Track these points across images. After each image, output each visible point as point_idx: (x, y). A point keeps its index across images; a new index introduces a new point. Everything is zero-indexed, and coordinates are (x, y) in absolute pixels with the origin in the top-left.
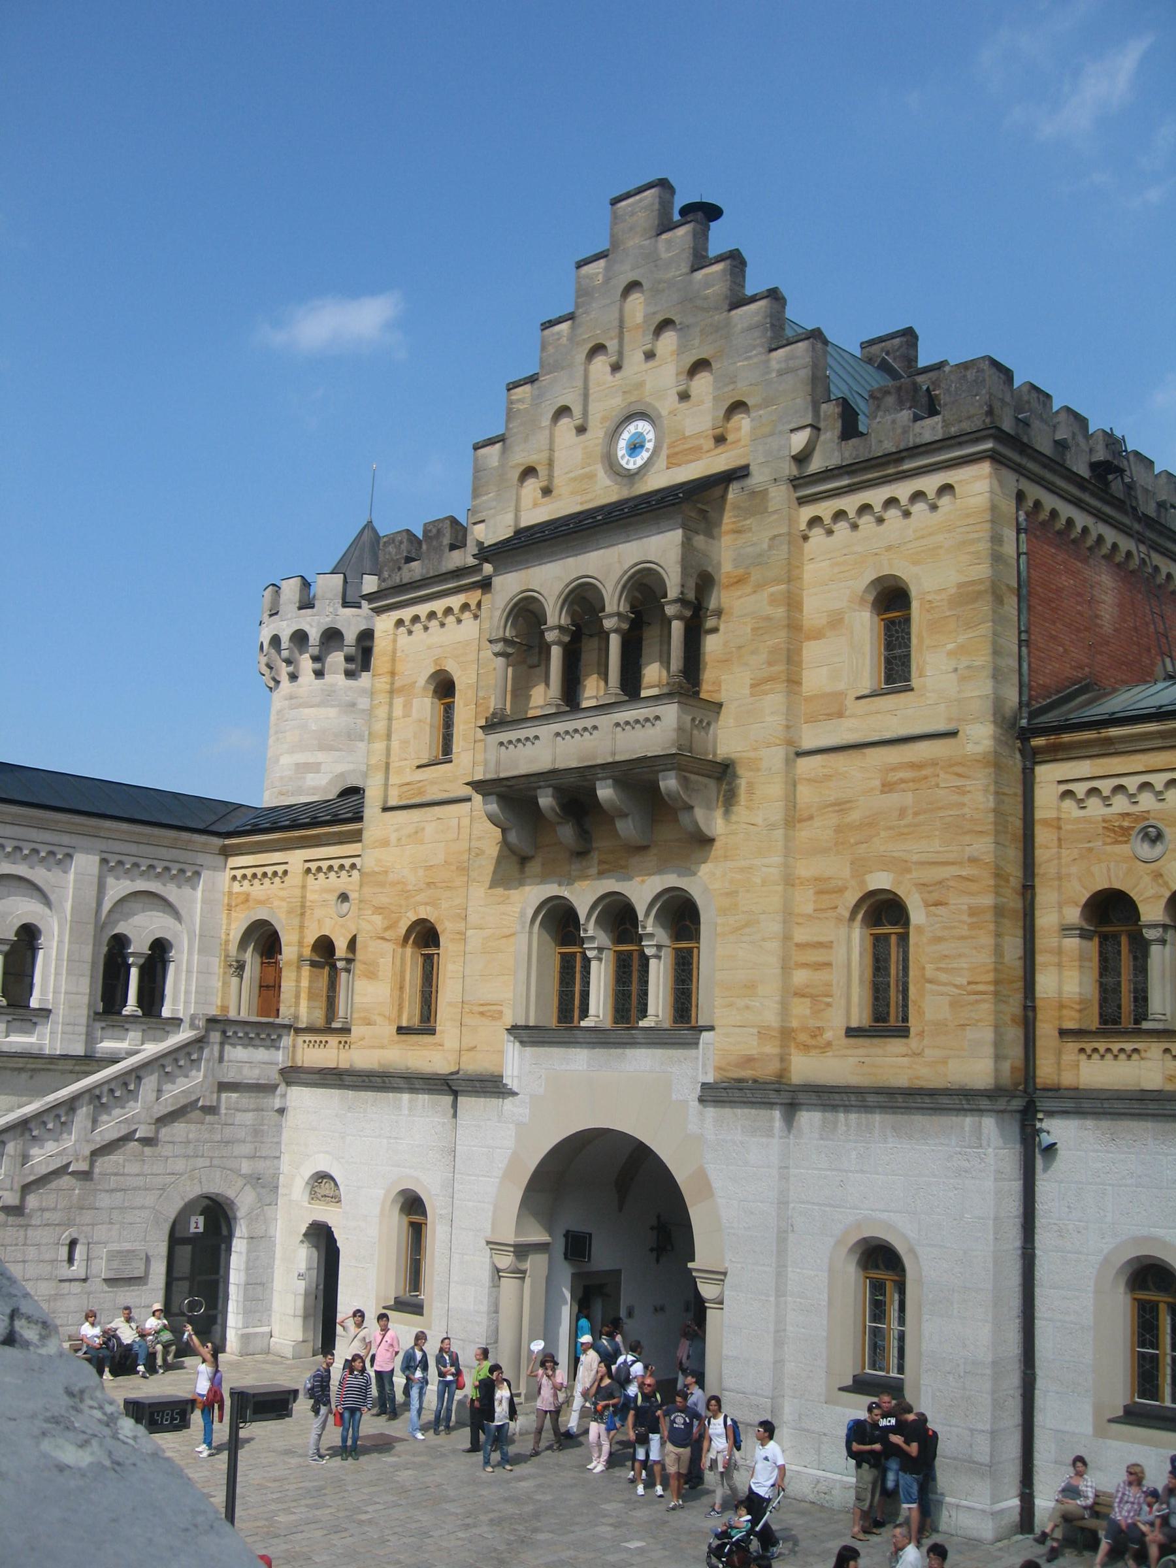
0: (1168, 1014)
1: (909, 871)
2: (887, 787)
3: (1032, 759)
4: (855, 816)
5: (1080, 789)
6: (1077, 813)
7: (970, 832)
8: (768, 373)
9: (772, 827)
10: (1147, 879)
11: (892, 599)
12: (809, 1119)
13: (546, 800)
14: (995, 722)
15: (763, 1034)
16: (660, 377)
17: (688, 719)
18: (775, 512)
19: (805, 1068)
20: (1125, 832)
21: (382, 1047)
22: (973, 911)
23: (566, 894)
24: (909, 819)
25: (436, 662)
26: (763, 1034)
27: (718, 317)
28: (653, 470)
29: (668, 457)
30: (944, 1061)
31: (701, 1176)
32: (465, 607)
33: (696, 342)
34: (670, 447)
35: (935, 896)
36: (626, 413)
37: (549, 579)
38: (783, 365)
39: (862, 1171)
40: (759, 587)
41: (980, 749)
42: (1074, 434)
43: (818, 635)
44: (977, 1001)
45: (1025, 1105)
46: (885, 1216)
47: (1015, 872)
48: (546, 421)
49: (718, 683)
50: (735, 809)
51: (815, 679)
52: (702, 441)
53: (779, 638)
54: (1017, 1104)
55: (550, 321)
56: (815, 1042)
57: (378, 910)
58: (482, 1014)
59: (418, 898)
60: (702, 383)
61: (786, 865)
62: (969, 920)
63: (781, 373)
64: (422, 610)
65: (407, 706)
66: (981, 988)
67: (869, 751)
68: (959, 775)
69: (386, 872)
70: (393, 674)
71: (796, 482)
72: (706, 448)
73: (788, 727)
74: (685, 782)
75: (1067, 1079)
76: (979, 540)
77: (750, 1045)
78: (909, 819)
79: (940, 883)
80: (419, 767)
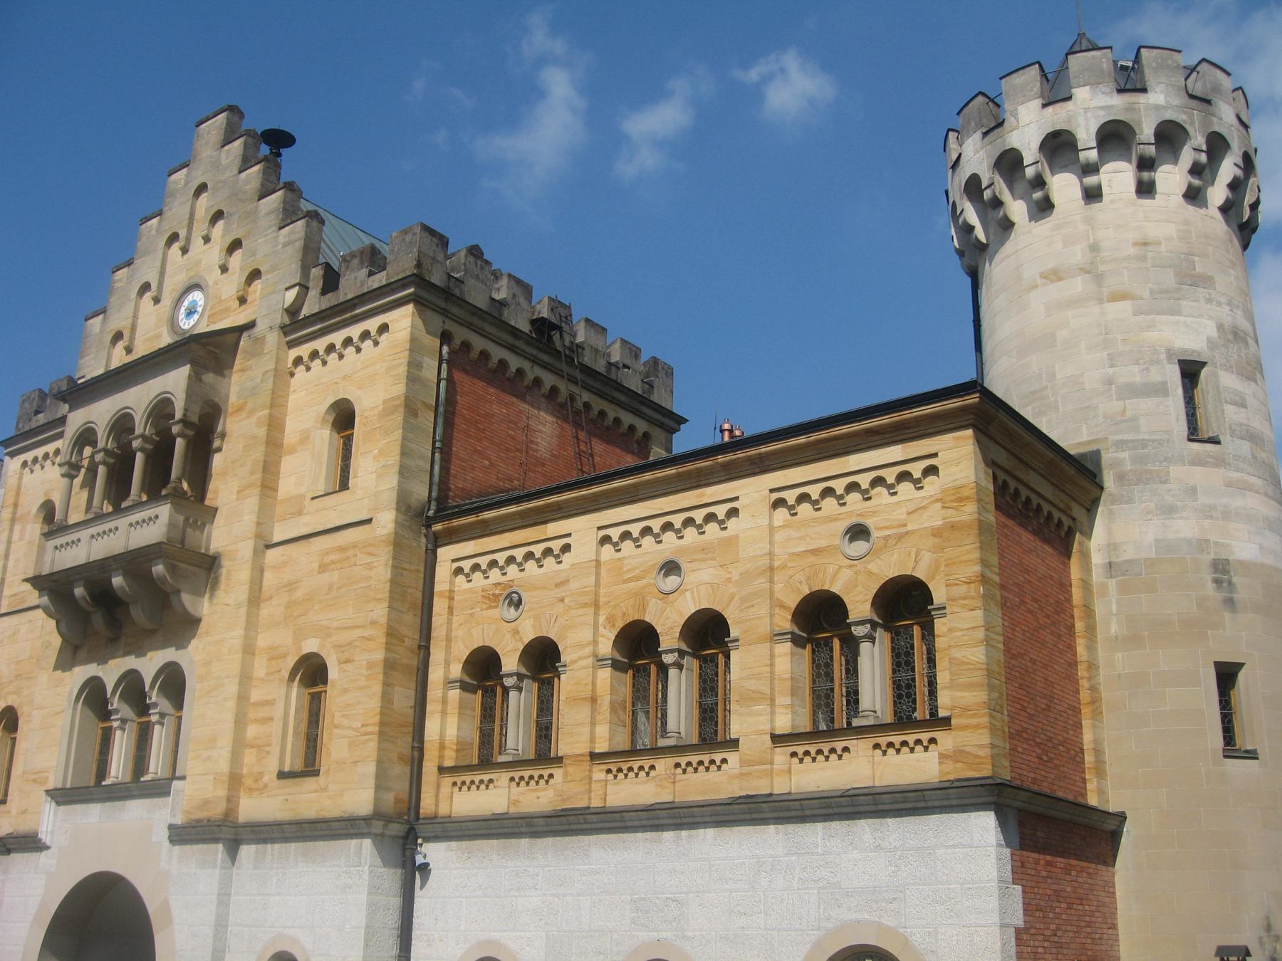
0: (520, 748)
1: (329, 636)
2: (323, 568)
3: (437, 541)
4: (299, 594)
6: (467, 586)
10: (508, 636)
12: (247, 852)
13: (79, 591)
14: (398, 510)
16: (207, 256)
17: (181, 518)
19: (251, 808)
22: (370, 666)
23: (100, 674)
25: (46, 494)
27: (250, 206)
31: (166, 905)
34: (212, 308)
36: (186, 285)
37: (100, 413)
39: (279, 894)
40: (251, 413)
41: (385, 532)
42: (514, 296)
44: (367, 741)
45: (403, 834)
47: (412, 636)
48: (134, 295)
49: (216, 492)
50: (217, 593)
51: (287, 485)
53: (259, 453)
54: (396, 829)
58: (34, 781)
60: (237, 259)
61: (246, 637)
62: (366, 673)
63: (285, 245)
65: (23, 531)
66: (370, 729)
67: (313, 540)
68: (370, 554)
70: (16, 505)
71: (285, 330)
73: (258, 524)
74: (172, 569)
75: (443, 810)
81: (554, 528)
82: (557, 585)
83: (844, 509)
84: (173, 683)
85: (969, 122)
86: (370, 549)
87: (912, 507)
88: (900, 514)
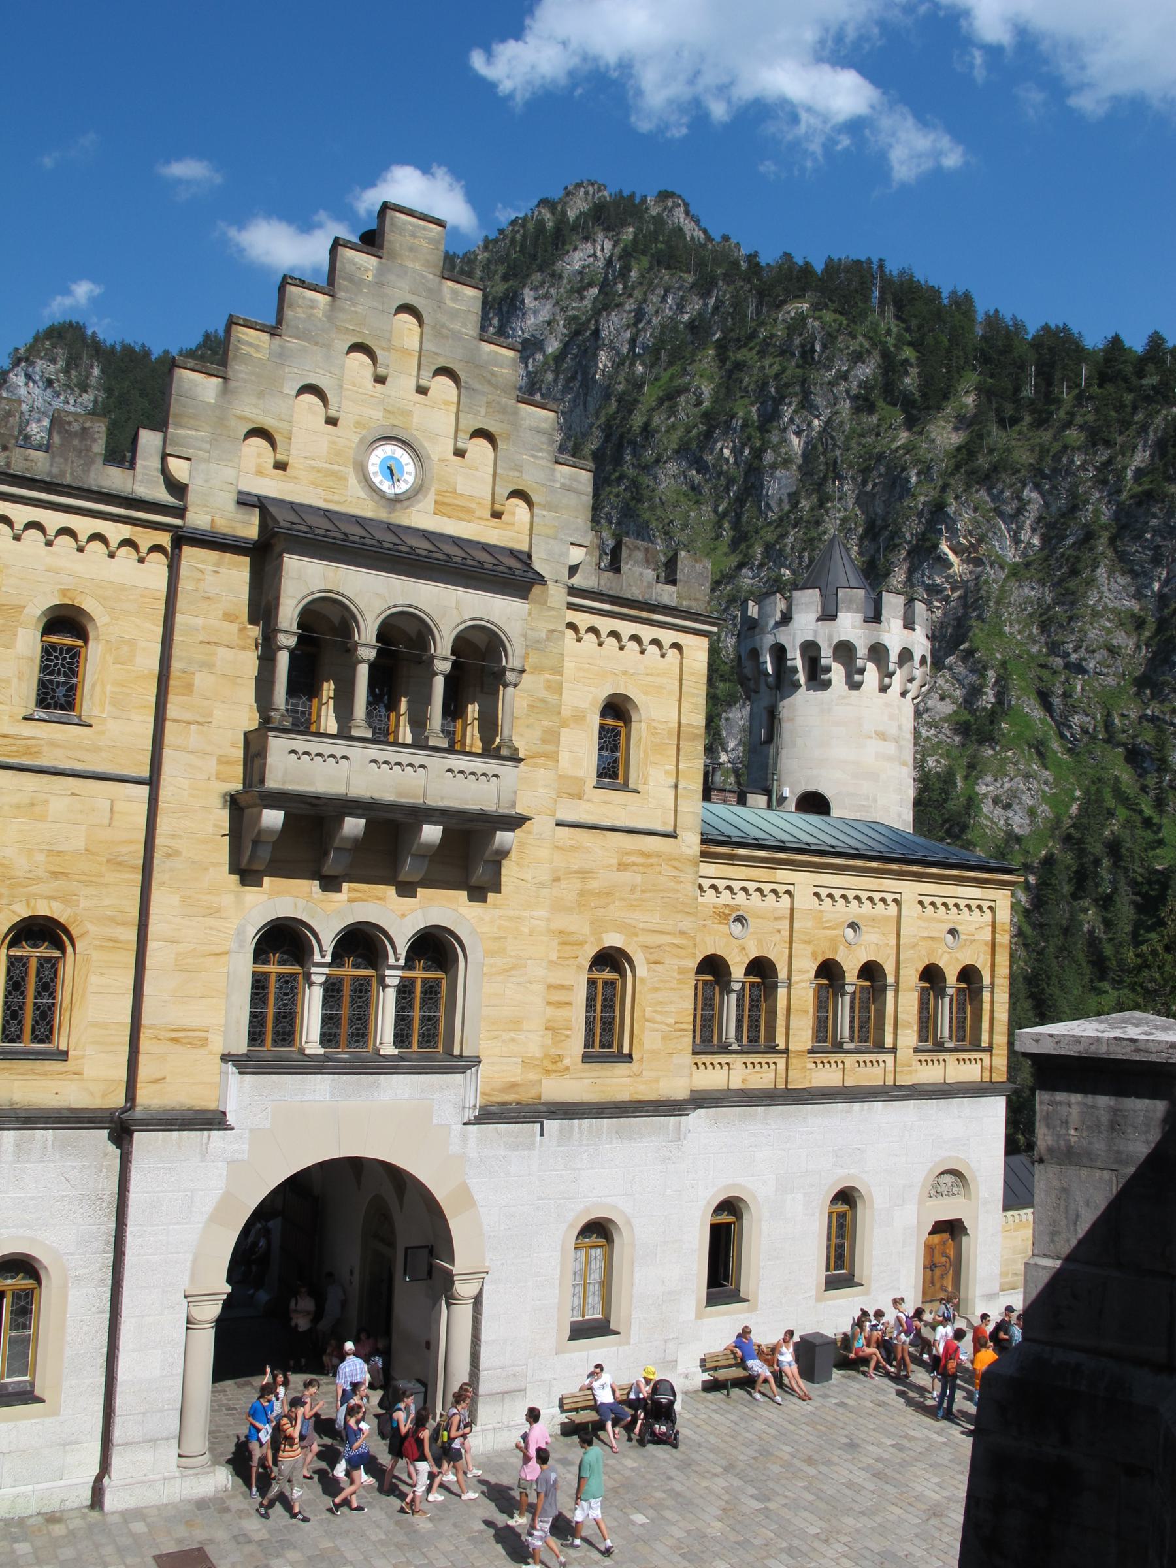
1: (636, 935)
2: (622, 867)
4: (594, 885)
7: (681, 911)
8: (554, 481)
9: (541, 885)
10: (736, 951)
11: (617, 710)
15: (526, 1063)
18: (553, 608)
20: (727, 916)
22: (681, 971)
24: (638, 895)
25: (64, 592)
26: (526, 1063)
28: (417, 507)
29: (436, 502)
30: (657, 1080)
32: (128, 543)
33: (483, 411)
38: (568, 482)
39: (592, 1168)
43: (564, 724)
46: (608, 1200)
48: (292, 388)
52: (473, 506)
55: (303, 282)
56: (553, 1065)
58: (175, 1040)
63: (566, 488)
64: (53, 520)
72: (478, 513)
76: (698, 695)
77: (511, 1071)
78: (638, 895)
79: (659, 947)
80: (24, 718)
81: (782, 875)
82: (776, 919)
83: (947, 917)
84: (435, 948)
85: (851, 601)
86: (676, 864)
87: (977, 925)
88: (972, 929)
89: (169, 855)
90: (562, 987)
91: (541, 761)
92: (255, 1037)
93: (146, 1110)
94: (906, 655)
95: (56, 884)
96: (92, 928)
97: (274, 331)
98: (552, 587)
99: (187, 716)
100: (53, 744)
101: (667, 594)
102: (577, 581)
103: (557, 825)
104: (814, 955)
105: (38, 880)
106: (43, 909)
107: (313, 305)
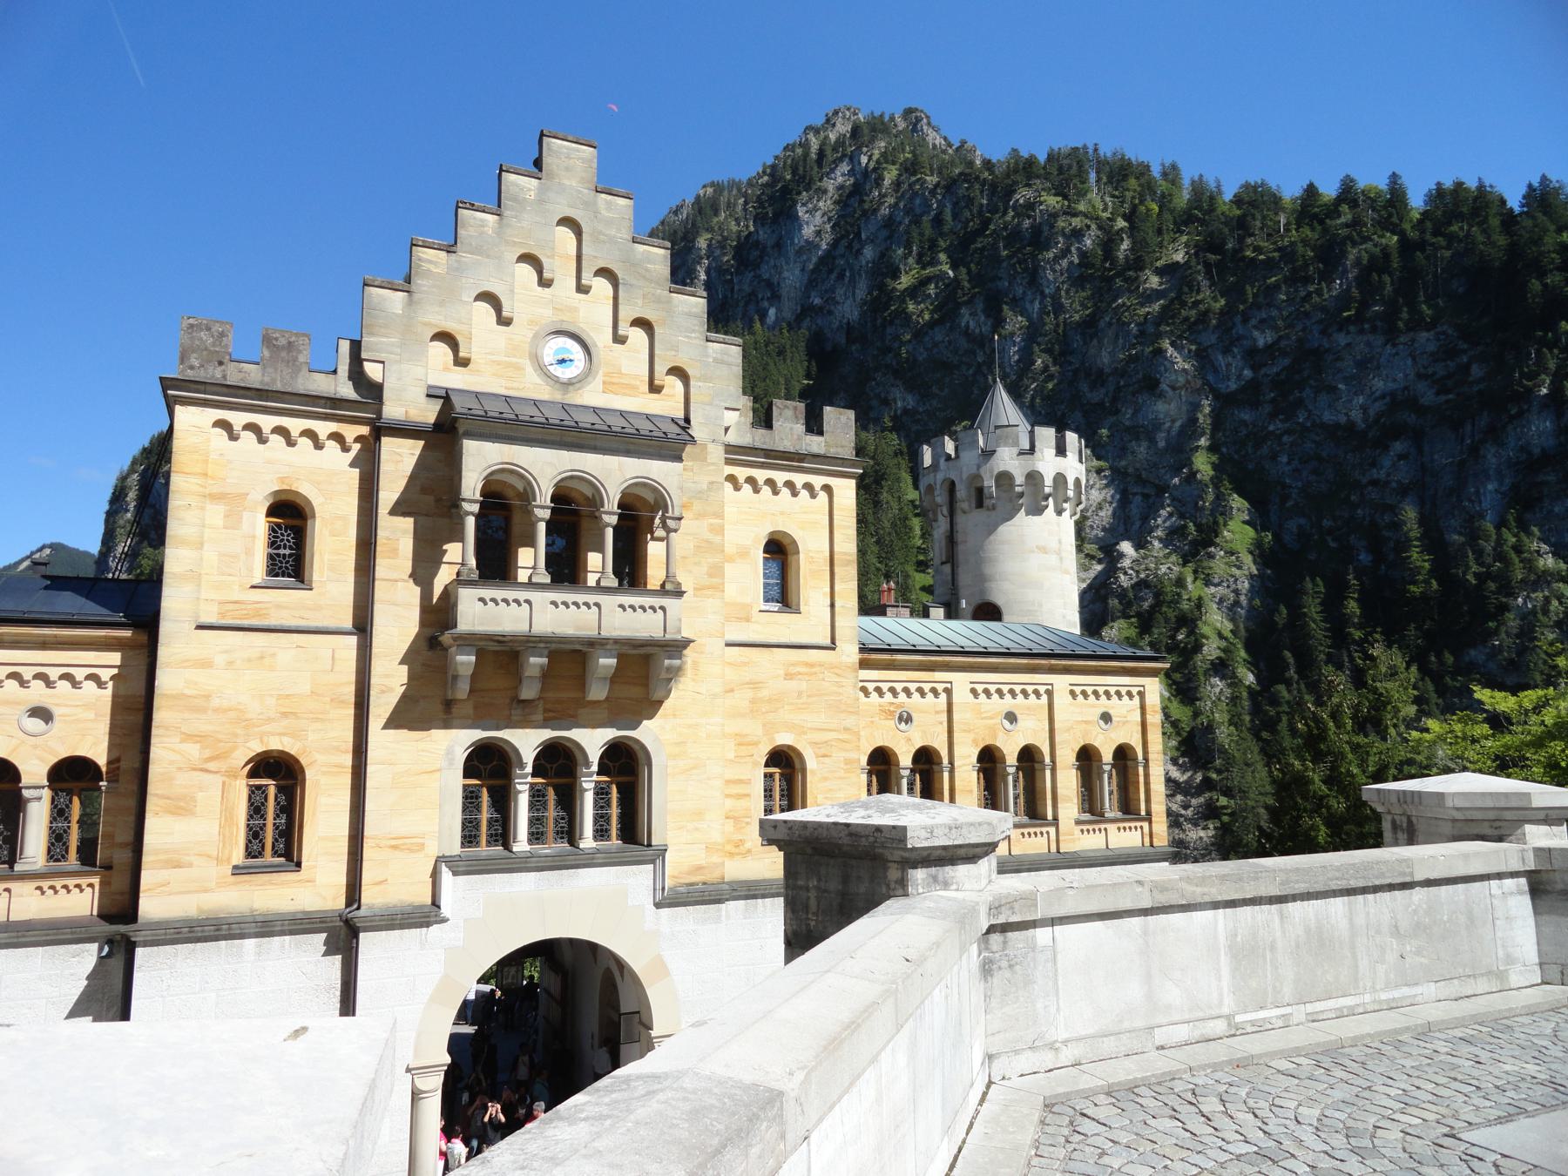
2: (789, 676)
4: (764, 693)
5: (871, 687)
11: (779, 550)
20: (892, 713)
21: (206, 891)
22: (848, 762)
25: (282, 480)
33: (640, 302)
35: (823, 751)
43: (731, 560)
51: (731, 591)
56: (736, 849)
57: (189, 737)
58: (395, 847)
59: (267, 728)
63: (716, 360)
69: (207, 697)
77: (699, 857)
88: (1124, 712)
89: (383, 692)
90: (740, 782)
91: (709, 592)
92: (469, 838)
93: (370, 907)
94: (1060, 479)
95: (285, 722)
96: (321, 758)
97: (450, 249)
98: (711, 447)
99: (395, 576)
100: (279, 606)
101: (815, 444)
102: (732, 438)
103: (728, 645)
104: (975, 741)
105: (269, 720)
106: (275, 744)
107: (483, 224)
